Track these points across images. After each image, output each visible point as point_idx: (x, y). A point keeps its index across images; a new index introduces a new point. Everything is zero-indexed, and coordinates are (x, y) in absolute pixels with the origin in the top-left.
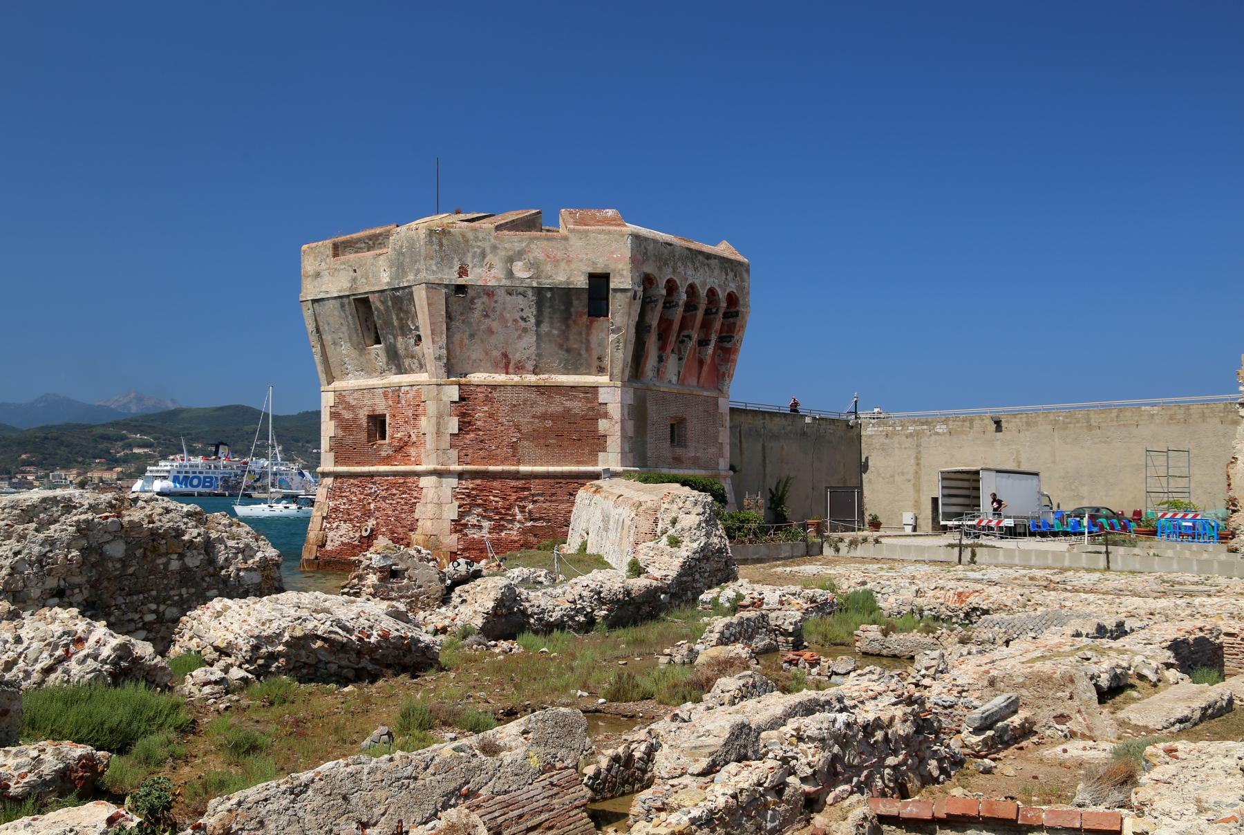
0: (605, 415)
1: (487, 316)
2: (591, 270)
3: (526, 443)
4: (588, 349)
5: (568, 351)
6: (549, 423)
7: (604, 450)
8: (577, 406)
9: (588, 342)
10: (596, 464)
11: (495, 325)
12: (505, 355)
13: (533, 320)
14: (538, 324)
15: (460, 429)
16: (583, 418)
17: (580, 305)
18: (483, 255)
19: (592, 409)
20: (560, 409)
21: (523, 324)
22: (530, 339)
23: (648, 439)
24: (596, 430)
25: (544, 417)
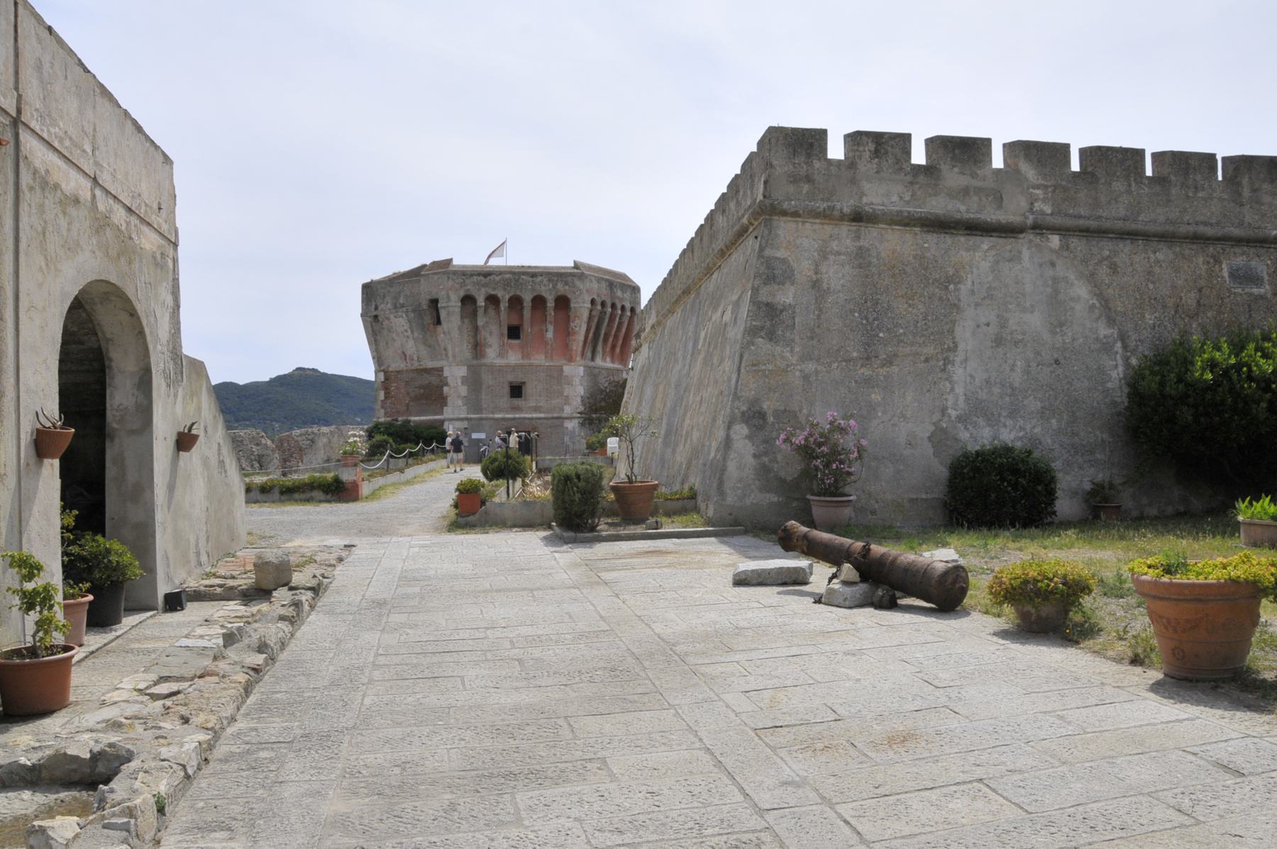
0: (447, 384)
1: (390, 331)
2: (429, 297)
3: (412, 403)
4: (439, 345)
5: (430, 347)
6: (422, 391)
7: (446, 405)
8: (434, 380)
9: (437, 341)
10: (442, 414)
11: (394, 335)
12: (403, 353)
13: (409, 331)
14: (412, 332)
15: (386, 398)
16: (437, 387)
17: (428, 319)
18: (384, 297)
19: (441, 381)
20: (427, 382)
21: (406, 334)
22: (411, 343)
23: (483, 397)
24: (442, 393)
25: (421, 387)
